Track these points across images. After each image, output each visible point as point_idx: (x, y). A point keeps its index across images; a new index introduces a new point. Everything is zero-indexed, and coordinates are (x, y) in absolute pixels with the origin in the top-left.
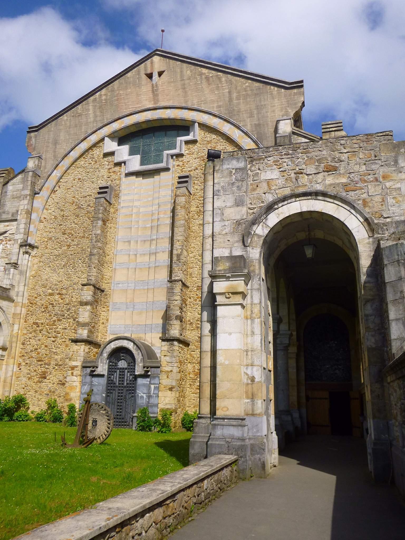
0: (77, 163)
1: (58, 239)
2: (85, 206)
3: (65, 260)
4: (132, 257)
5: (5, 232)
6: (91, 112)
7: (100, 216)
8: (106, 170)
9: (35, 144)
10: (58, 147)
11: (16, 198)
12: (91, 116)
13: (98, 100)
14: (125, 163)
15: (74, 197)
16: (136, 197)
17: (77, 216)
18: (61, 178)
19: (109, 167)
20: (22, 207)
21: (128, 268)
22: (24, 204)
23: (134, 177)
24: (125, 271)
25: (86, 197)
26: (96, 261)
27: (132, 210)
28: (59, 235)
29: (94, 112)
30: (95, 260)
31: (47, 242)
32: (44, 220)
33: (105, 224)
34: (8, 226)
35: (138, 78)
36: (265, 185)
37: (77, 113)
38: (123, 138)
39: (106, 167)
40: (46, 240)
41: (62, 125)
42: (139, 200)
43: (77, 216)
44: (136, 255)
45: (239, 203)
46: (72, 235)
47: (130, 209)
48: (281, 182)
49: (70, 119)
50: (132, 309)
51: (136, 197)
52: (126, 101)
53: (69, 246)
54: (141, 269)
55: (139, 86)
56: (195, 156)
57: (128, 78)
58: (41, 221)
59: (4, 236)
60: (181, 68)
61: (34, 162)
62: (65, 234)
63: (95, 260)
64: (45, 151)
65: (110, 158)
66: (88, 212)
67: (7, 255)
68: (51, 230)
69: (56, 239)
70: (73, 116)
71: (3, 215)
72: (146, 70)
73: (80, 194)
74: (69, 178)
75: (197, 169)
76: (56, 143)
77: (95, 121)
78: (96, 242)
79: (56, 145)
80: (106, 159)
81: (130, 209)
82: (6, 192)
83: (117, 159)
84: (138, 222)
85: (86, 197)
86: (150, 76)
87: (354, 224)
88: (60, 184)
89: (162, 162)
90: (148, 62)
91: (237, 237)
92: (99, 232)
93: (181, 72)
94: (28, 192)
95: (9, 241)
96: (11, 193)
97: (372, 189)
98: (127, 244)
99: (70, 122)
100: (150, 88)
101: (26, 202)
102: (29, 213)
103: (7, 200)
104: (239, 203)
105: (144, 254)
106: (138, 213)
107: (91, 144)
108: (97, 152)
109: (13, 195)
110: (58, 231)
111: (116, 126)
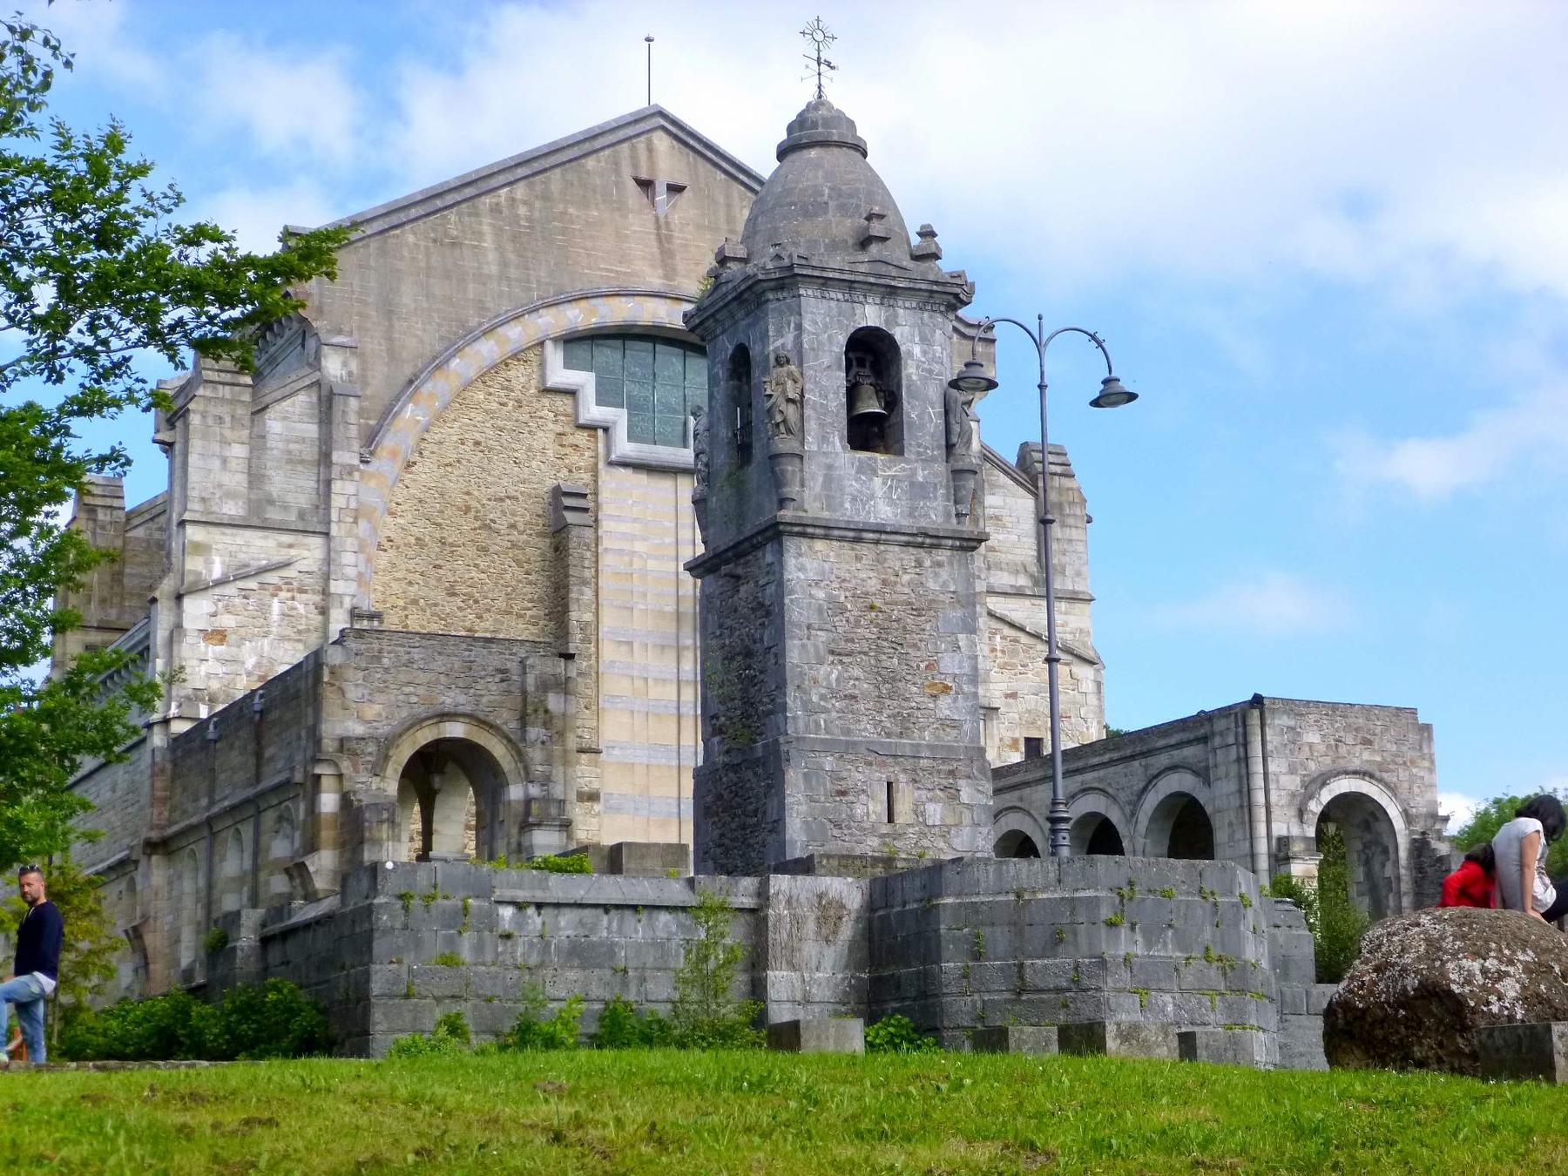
0: (467, 394)
1: (436, 605)
4: (639, 684)
5: (287, 565)
6: (488, 243)
8: (553, 436)
9: (321, 295)
10: (397, 324)
11: (302, 462)
12: (492, 256)
13: (505, 211)
14: (606, 430)
15: (468, 493)
16: (636, 528)
17: (484, 550)
19: (559, 429)
21: (632, 712)
23: (628, 472)
24: (626, 719)
25: (501, 500)
27: (631, 564)
28: (439, 596)
29: (499, 248)
31: (405, 609)
32: (387, 545)
34: (290, 546)
35: (617, 184)
37: (446, 235)
38: (578, 342)
39: (551, 426)
40: (401, 603)
41: (402, 258)
42: (645, 539)
43: (484, 550)
44: (646, 679)
45: (1292, 771)
46: (476, 602)
47: (626, 559)
48: (1322, 748)
49: (427, 248)
50: (646, 813)
51: (636, 528)
52: (589, 244)
54: (657, 715)
55: (621, 208)
57: (588, 172)
58: (380, 547)
59: (285, 573)
60: (728, 196)
61: (345, 364)
62: (454, 594)
64: (359, 328)
65: (563, 403)
66: (514, 545)
67: (299, 632)
68: (410, 577)
69: (430, 606)
70: (435, 241)
71: (270, 508)
72: (635, 166)
73: (483, 489)
74: (451, 432)
76: (389, 310)
77: (503, 276)
78: (583, 641)
79: (390, 320)
80: (546, 401)
81: (626, 559)
82: (264, 437)
84: (645, 595)
85: (501, 500)
86: (646, 185)
87: (1394, 812)
88: (423, 445)
90: (641, 144)
91: (1293, 812)
93: (729, 206)
95: (301, 591)
96: (280, 445)
97: (1404, 775)
98: (624, 649)
99: (428, 255)
100: (651, 227)
103: (269, 464)
104: (1292, 771)
105: (664, 680)
106: (644, 572)
107: (509, 349)
108: (519, 375)
109: (289, 452)
111: (578, 317)
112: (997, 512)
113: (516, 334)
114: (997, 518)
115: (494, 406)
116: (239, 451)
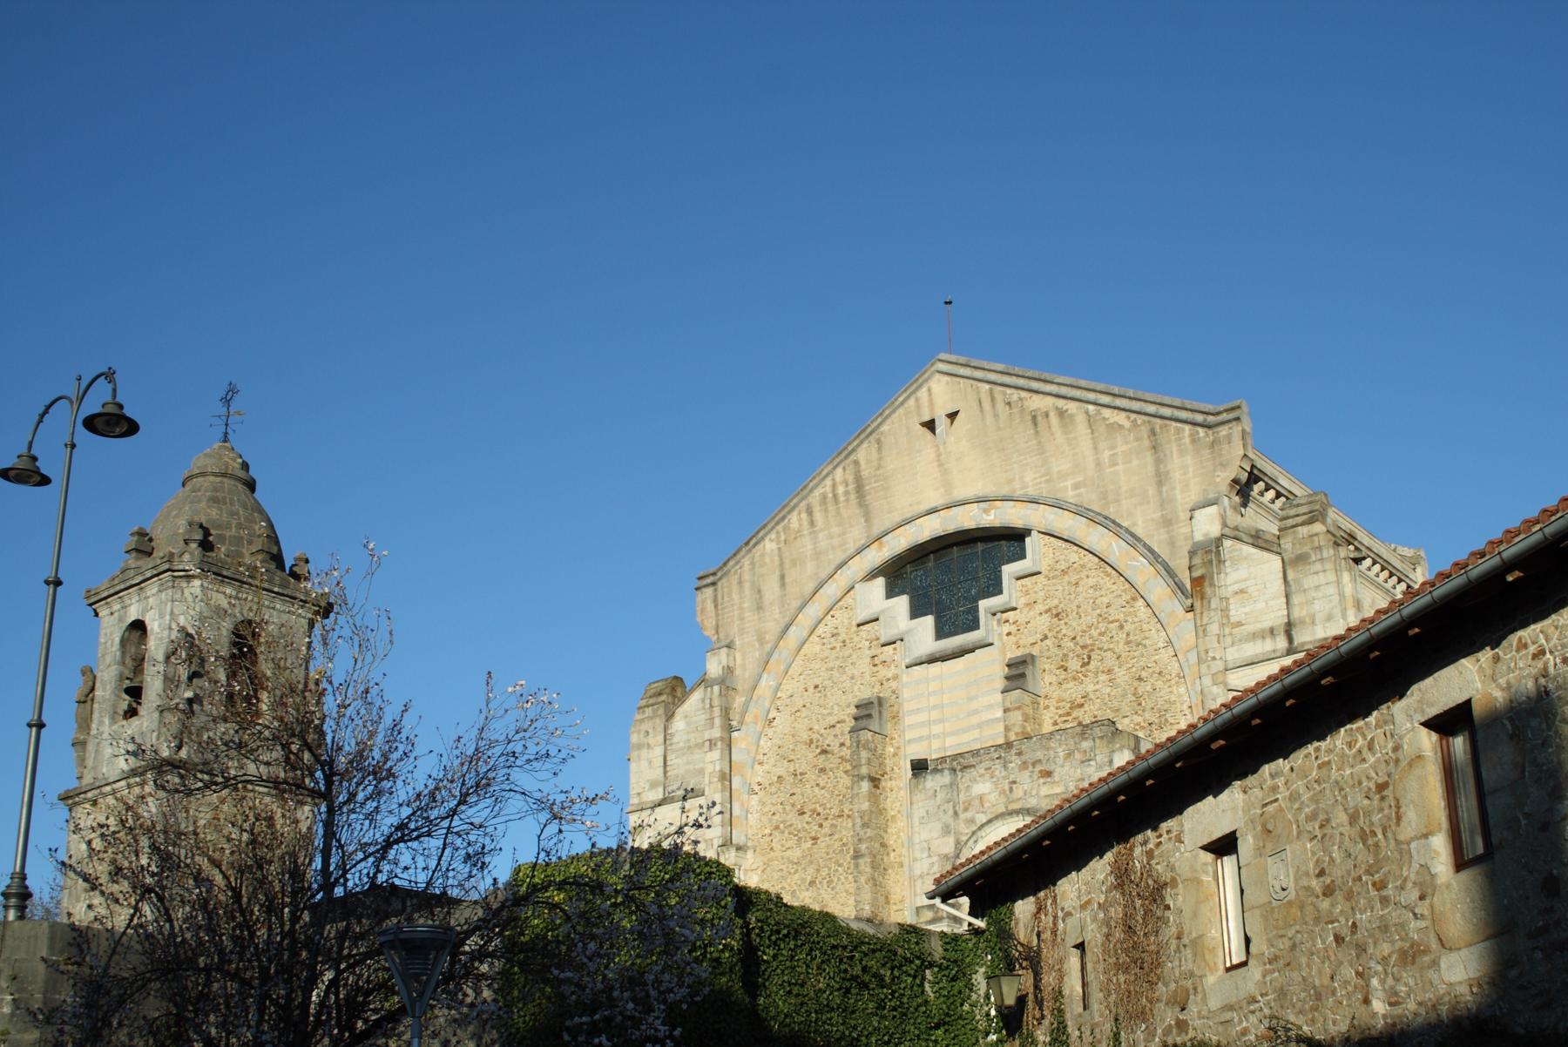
2: (836, 749)
3: (811, 870)
7: (864, 770)
16: (935, 715)
17: (822, 770)
18: (777, 689)
20: (709, 768)
22: (713, 760)
26: (869, 870)
28: (792, 817)
30: (865, 863)
33: (876, 787)
36: (977, 803)
40: (767, 831)
43: (822, 770)
47: (925, 743)
48: (993, 797)
51: (935, 715)
53: (815, 839)
56: (1040, 607)
63: (865, 863)
75: (1046, 637)
83: (884, 631)
86: (930, 425)
89: (977, 627)
92: (865, 806)
94: (716, 733)
101: (715, 755)
102: (726, 778)
107: (826, 603)
108: (841, 618)
110: (788, 808)
112: (1242, 585)
113: (832, 590)
114: (1242, 591)
115: (827, 652)
116: (659, 751)
